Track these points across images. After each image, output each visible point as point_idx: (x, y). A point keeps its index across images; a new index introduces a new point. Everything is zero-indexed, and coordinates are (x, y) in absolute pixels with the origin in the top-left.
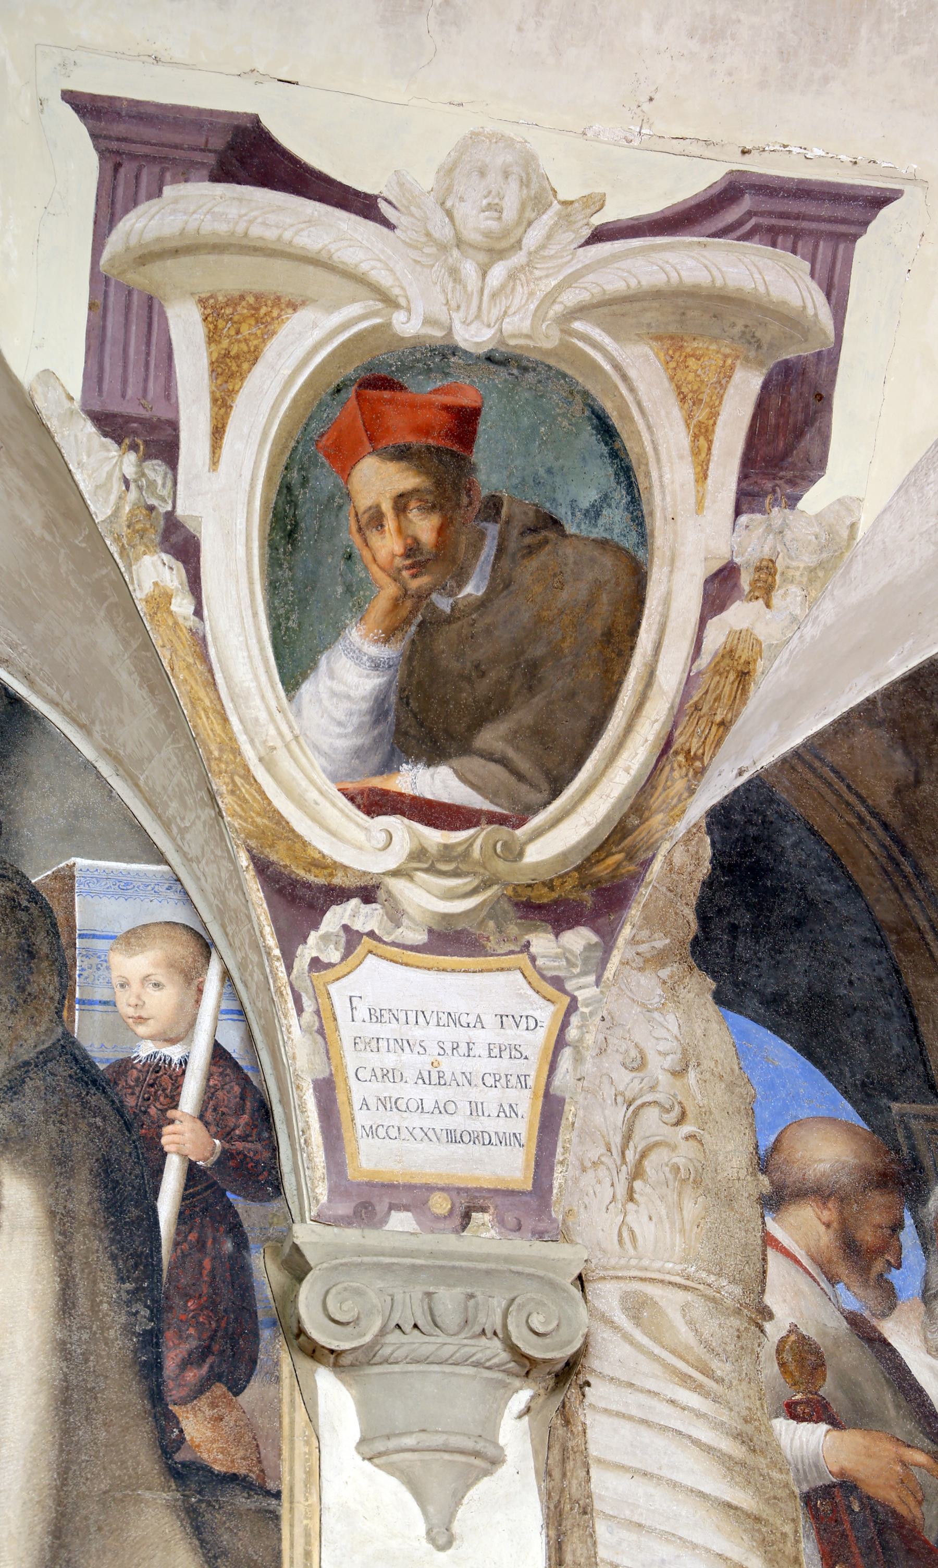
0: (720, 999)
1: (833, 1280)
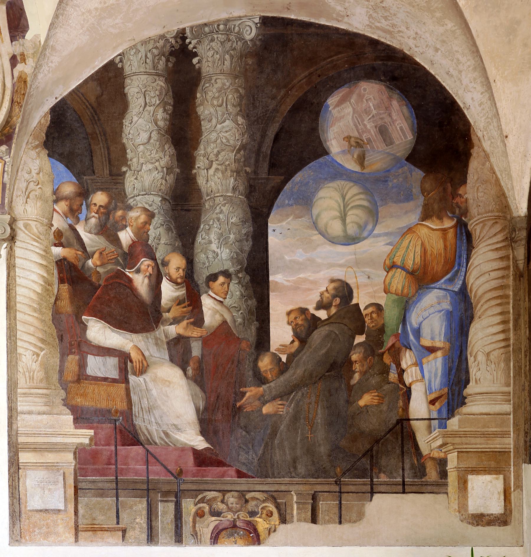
1: (67, 217)
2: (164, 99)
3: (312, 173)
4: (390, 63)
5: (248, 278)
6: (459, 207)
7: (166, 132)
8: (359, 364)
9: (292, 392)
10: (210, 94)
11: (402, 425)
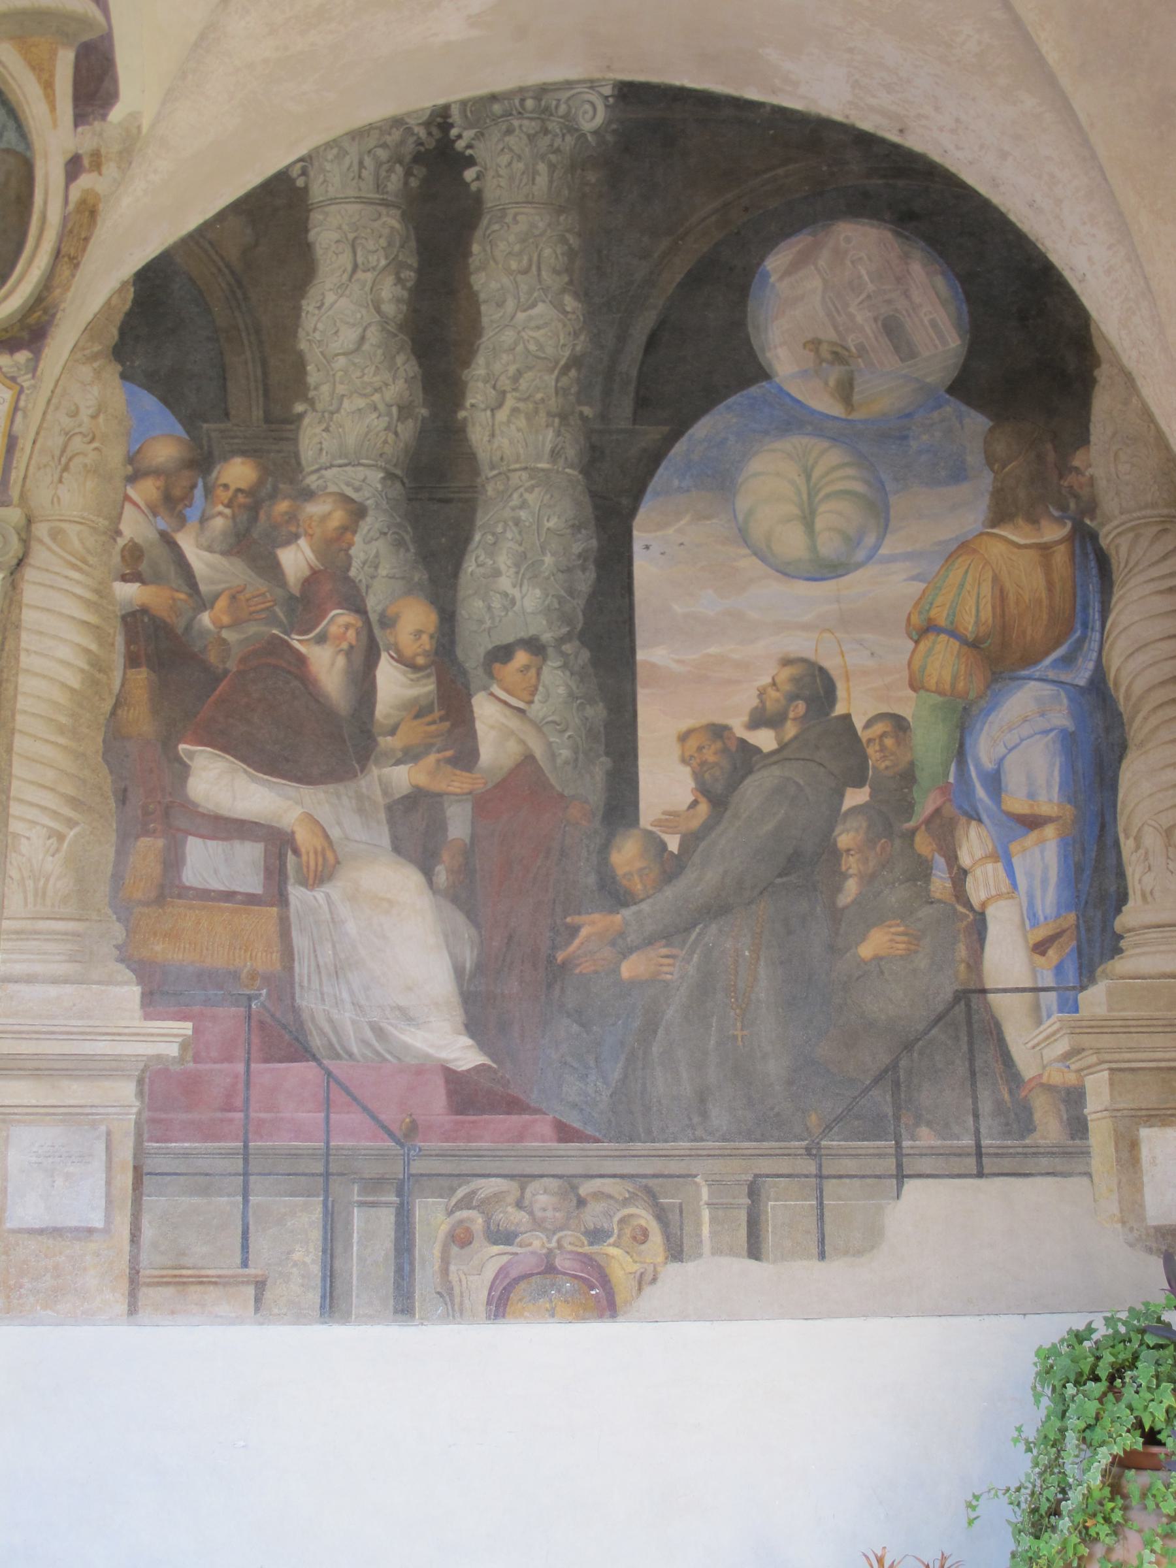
0: (124, 376)
1: (155, 515)
2: (397, 256)
3: (734, 420)
4: (901, 183)
5: (585, 655)
6: (1076, 496)
7: (401, 327)
8: (857, 856)
9: (695, 926)
10: (502, 245)
11: (968, 1005)
